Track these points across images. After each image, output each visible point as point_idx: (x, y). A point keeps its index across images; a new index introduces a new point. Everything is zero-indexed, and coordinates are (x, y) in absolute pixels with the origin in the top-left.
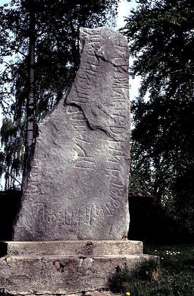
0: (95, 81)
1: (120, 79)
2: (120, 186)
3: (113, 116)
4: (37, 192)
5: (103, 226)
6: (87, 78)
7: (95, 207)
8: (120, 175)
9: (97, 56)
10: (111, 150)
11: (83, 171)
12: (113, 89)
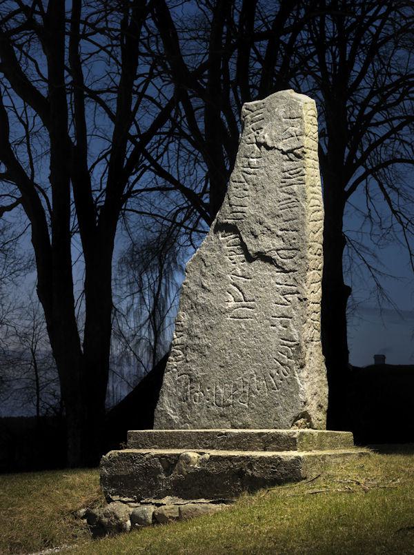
0: (255, 182)
1: (292, 172)
2: (290, 343)
3: (280, 233)
4: (183, 359)
5: (265, 407)
6: (243, 180)
7: (255, 378)
8: (291, 326)
9: (259, 144)
10: (278, 286)
11: (239, 323)
12: (280, 189)
